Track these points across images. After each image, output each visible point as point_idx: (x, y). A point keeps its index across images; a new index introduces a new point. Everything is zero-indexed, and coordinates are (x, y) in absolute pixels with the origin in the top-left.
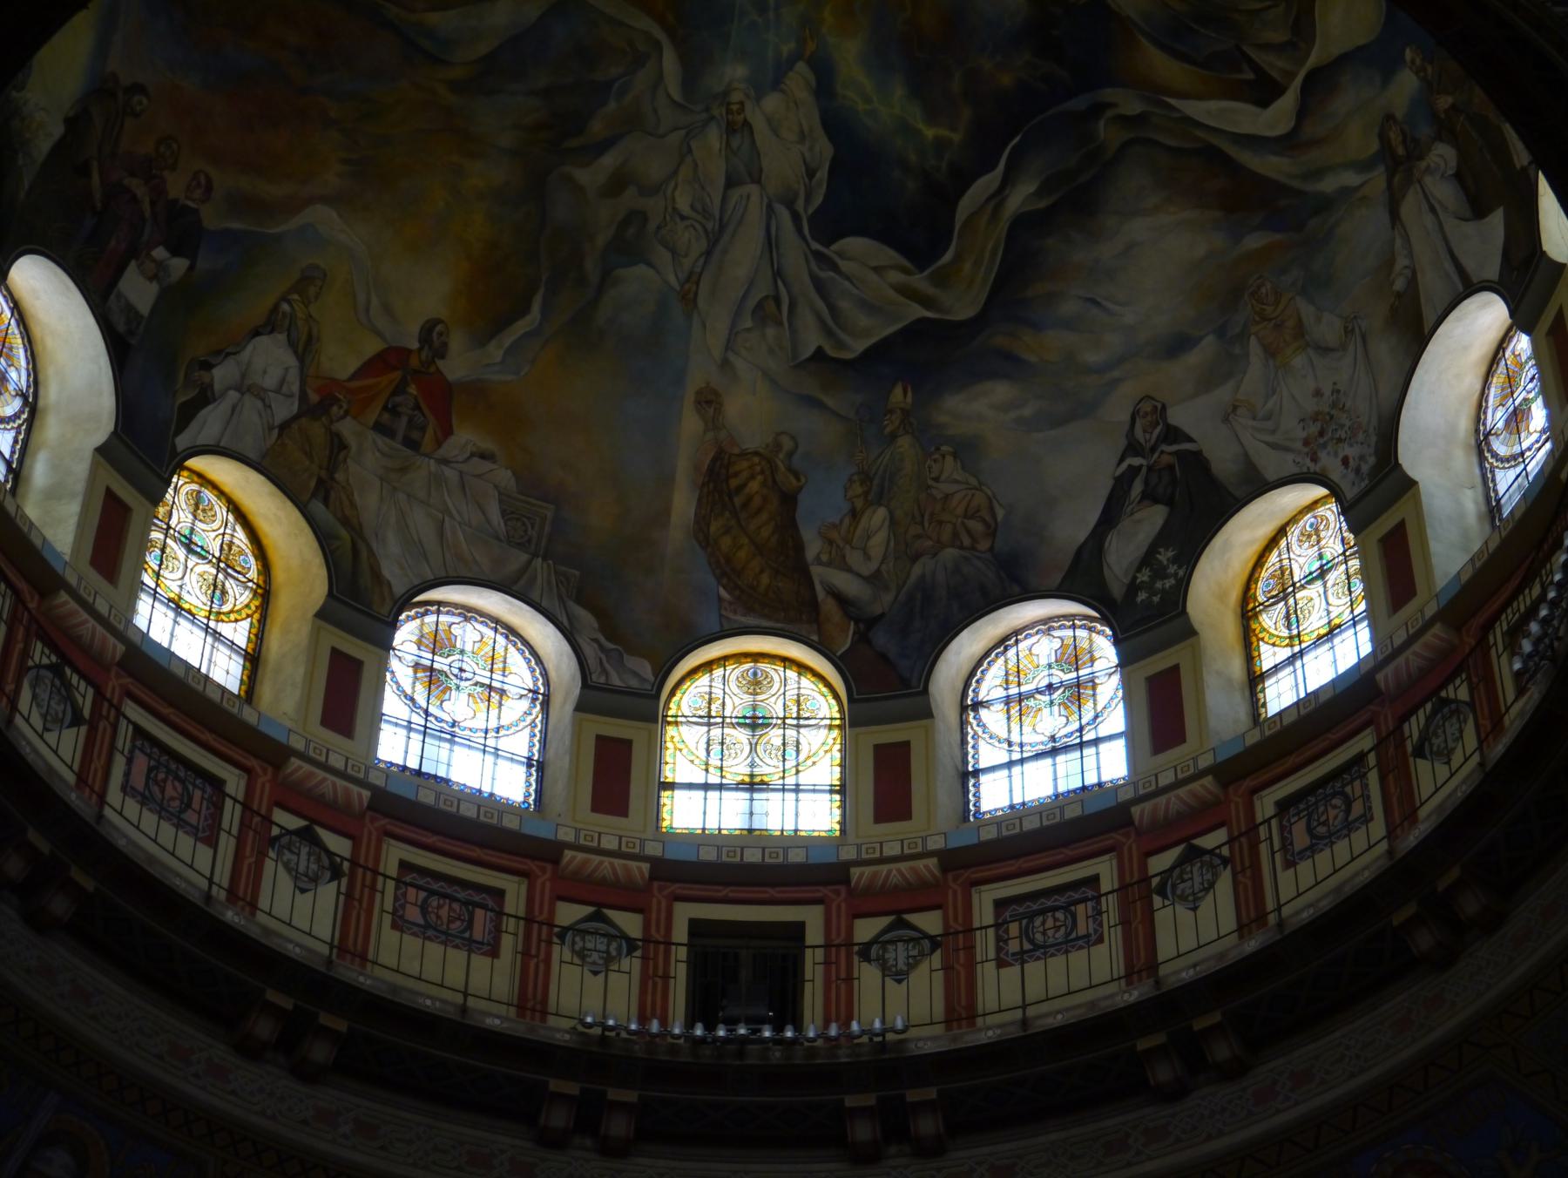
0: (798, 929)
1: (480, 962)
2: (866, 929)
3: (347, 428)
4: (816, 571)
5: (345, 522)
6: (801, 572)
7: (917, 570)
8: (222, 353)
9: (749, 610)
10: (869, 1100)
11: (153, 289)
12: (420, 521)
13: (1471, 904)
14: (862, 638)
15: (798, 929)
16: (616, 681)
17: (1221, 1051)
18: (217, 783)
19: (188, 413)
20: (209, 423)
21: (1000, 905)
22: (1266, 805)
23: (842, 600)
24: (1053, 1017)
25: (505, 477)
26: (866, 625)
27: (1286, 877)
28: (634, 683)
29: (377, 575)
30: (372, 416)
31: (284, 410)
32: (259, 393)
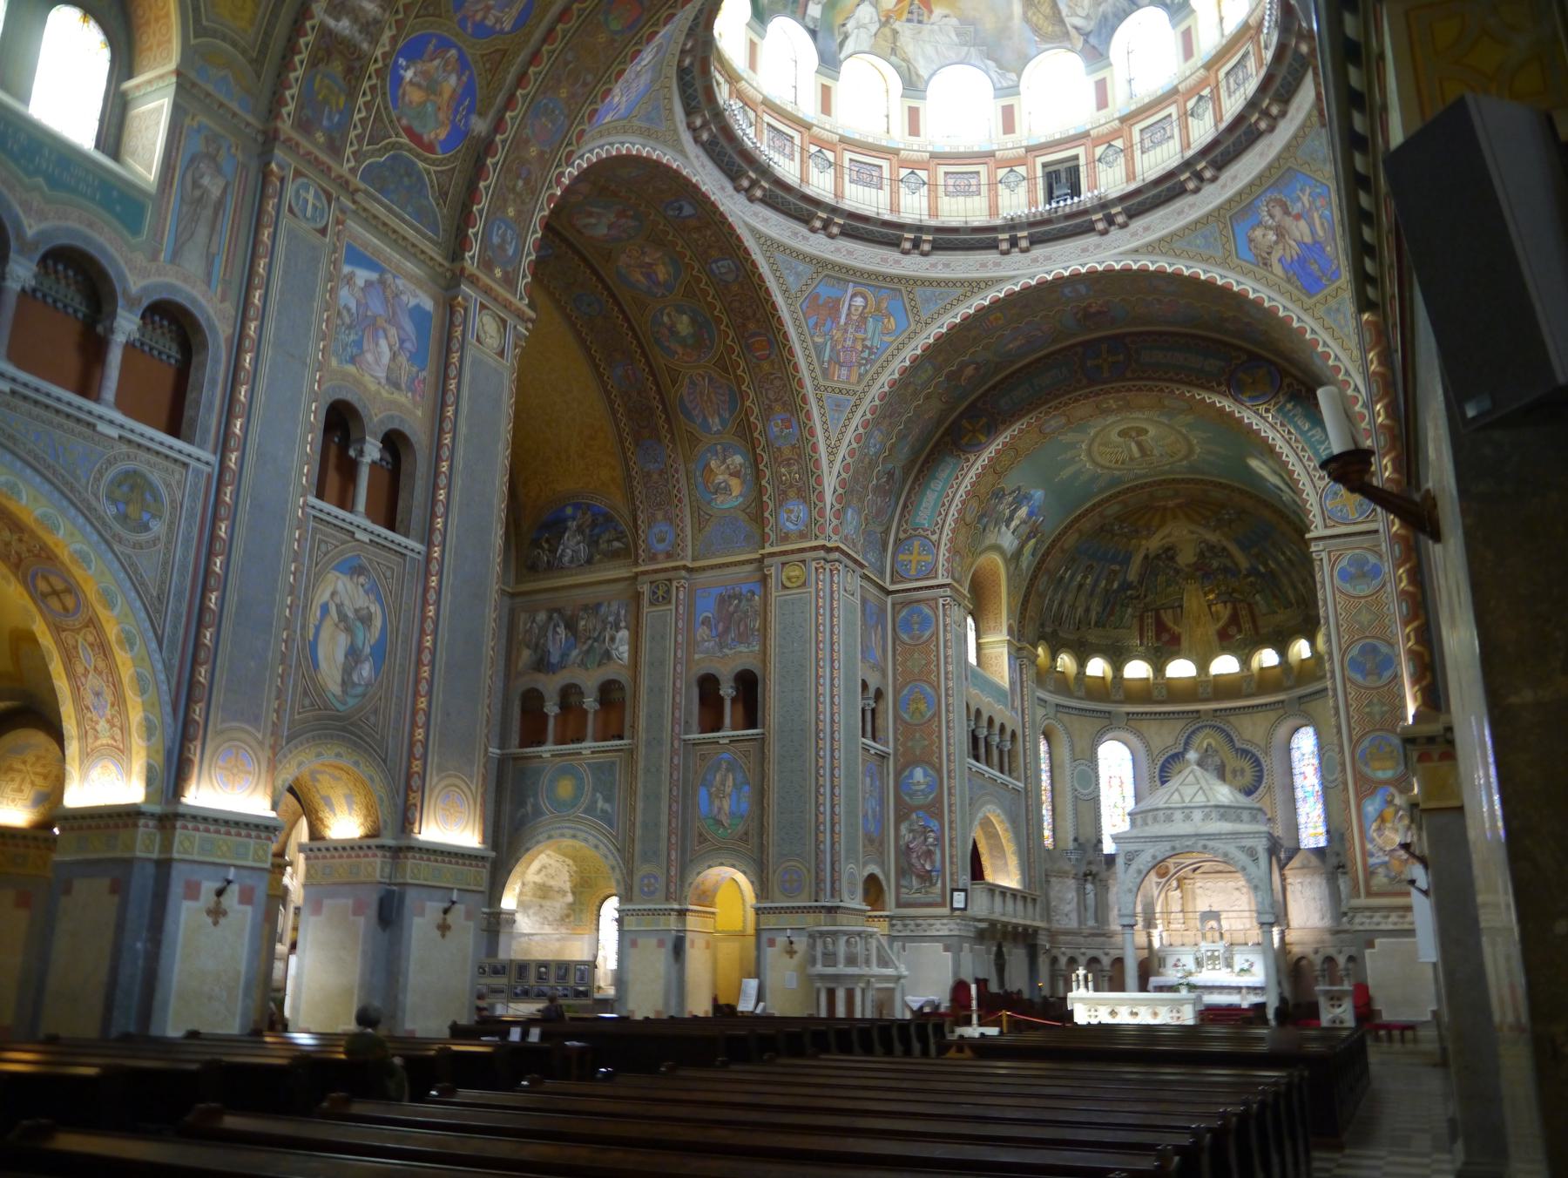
0: (1076, 158)
1: (977, 198)
2: (1099, 151)
3: (897, 25)
4: (1067, 20)
5: (904, 60)
6: (1062, 22)
7: (1101, 9)
8: (848, 18)
9: (1046, 42)
10: (1100, 216)
11: (820, 7)
12: (929, 50)
13: (1275, 110)
14: (1086, 41)
15: (1076, 158)
16: (1005, 85)
17: (1208, 174)
18: (880, 167)
19: (842, 44)
20: (850, 46)
21: (1142, 131)
22: (1222, 74)
23: (1076, 28)
24: (1152, 175)
25: (954, 21)
26: (1086, 35)
27: (1228, 102)
28: (1011, 83)
29: (918, 75)
30: (904, 17)
31: (874, 28)
32: (864, 26)
